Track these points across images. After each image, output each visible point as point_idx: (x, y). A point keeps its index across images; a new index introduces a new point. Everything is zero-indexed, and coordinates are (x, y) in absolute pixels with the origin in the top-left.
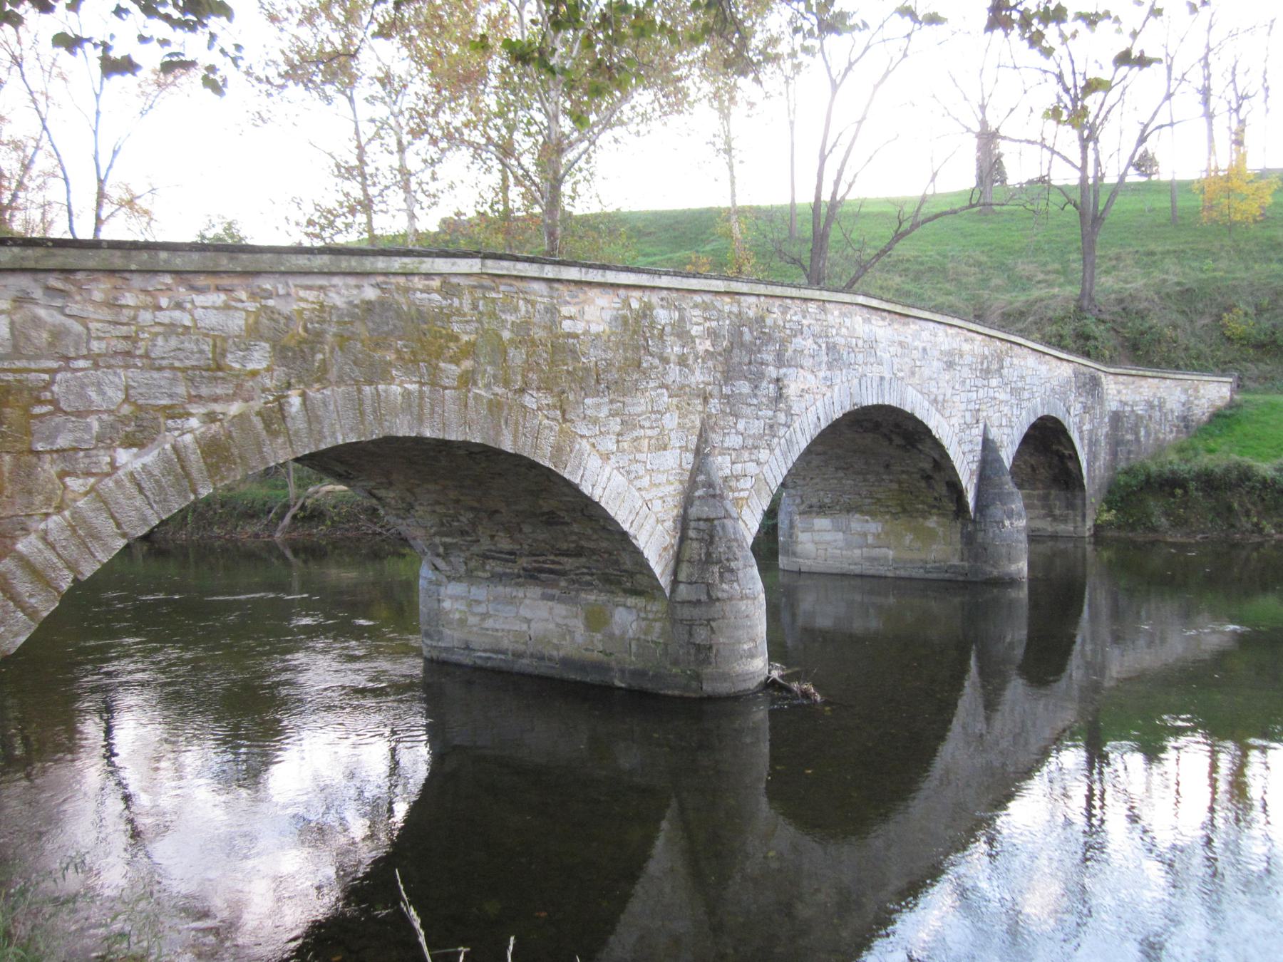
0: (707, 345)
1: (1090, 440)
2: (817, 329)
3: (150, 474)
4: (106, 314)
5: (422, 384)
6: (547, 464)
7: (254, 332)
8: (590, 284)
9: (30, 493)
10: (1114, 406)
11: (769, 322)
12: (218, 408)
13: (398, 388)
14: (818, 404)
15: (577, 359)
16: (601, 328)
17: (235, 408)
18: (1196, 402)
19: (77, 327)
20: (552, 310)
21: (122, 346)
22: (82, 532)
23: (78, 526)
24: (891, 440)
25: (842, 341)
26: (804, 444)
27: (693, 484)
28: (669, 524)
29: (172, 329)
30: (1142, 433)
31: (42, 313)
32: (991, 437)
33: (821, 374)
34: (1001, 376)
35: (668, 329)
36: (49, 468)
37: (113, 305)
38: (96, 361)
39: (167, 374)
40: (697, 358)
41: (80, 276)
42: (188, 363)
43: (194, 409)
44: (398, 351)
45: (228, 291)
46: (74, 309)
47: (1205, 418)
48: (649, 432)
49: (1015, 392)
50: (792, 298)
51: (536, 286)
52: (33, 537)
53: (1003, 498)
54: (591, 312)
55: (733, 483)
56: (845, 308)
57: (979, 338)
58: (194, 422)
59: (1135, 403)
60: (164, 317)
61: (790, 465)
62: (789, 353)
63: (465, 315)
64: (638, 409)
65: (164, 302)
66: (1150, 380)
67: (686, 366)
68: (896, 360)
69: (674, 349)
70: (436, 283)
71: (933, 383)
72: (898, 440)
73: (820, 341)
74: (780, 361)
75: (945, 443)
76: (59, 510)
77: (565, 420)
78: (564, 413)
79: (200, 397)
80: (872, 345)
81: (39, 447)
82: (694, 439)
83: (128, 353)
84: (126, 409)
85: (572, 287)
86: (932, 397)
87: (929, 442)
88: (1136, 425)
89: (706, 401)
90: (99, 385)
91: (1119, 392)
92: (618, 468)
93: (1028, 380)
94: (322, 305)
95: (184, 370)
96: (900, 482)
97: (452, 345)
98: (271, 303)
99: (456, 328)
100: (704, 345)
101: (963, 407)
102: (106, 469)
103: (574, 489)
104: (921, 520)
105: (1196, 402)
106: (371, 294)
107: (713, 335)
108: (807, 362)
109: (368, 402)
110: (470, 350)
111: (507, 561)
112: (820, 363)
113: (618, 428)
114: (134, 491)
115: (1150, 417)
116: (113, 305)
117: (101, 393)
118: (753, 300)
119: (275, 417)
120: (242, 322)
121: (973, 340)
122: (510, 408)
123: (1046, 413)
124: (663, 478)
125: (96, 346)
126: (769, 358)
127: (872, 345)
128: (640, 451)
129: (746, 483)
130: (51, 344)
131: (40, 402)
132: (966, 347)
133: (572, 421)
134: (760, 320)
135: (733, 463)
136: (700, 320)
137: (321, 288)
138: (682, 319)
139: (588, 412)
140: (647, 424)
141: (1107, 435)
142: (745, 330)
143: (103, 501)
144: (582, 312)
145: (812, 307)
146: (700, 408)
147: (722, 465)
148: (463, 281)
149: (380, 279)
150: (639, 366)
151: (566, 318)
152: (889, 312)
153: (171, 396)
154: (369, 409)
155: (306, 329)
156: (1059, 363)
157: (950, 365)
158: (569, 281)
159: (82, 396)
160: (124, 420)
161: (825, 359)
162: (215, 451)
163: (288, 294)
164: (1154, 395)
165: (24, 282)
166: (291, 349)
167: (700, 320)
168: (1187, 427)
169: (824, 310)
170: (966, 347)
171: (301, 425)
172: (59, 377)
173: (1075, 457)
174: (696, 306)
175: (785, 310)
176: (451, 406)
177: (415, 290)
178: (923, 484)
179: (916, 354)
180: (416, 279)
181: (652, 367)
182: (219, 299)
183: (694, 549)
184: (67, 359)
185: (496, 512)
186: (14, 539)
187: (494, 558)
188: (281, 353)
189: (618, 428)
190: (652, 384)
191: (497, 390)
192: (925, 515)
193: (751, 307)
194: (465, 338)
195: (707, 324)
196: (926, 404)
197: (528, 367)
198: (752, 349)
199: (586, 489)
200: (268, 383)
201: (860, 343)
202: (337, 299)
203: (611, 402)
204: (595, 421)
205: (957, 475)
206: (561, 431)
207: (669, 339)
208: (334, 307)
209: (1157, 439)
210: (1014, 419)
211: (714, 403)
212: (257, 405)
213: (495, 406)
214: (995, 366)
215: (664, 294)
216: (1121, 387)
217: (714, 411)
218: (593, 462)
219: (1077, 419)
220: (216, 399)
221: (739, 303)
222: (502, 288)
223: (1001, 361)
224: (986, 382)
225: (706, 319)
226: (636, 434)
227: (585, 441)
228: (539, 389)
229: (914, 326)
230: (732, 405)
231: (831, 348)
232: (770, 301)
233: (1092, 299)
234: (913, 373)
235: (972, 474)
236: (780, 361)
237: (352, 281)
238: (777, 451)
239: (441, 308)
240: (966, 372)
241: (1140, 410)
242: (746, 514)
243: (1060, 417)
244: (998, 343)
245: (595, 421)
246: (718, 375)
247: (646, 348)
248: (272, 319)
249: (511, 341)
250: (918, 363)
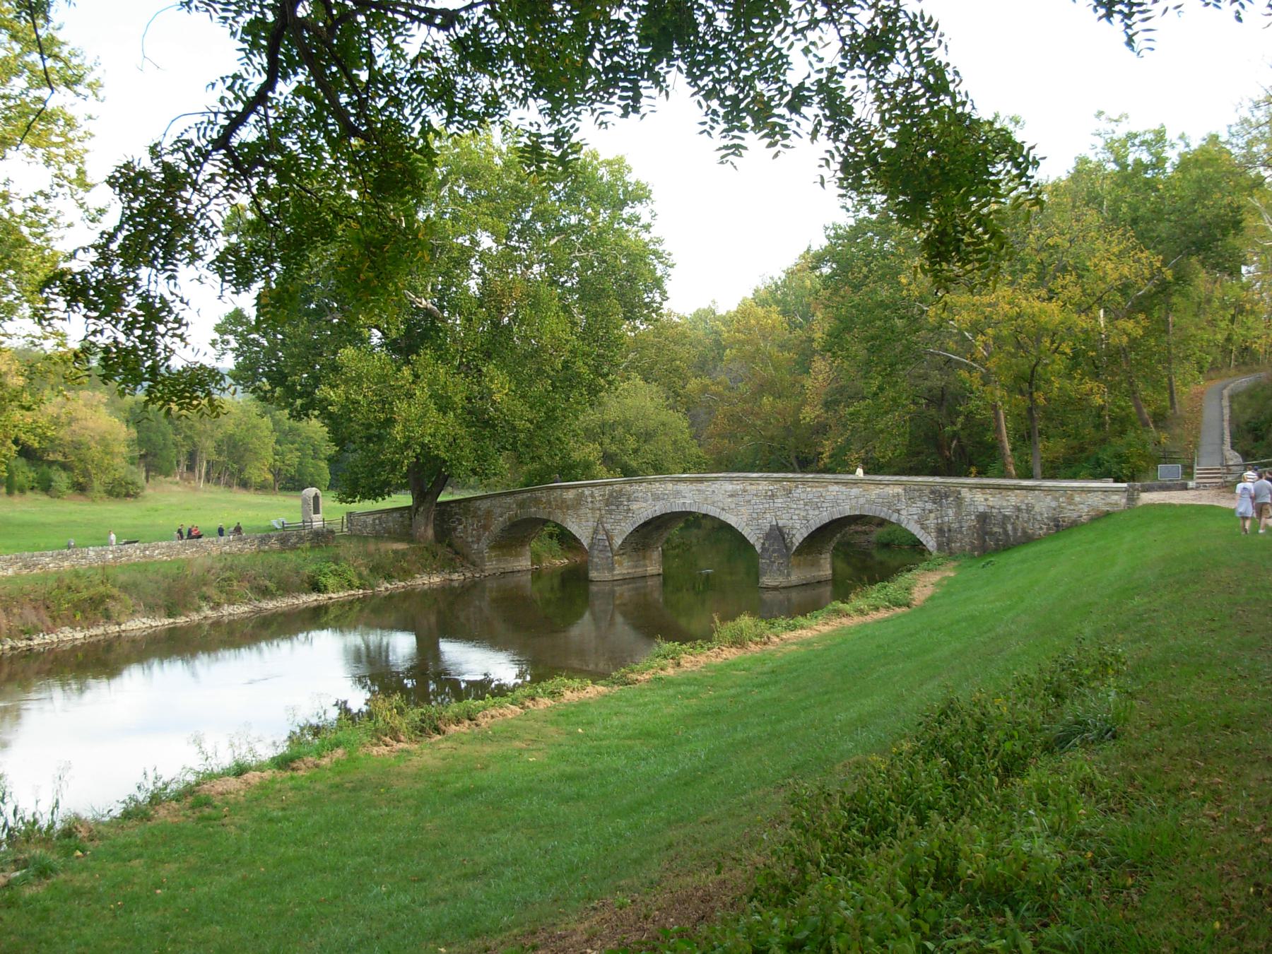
1: (940, 531)
10: (981, 509)
13: (533, 509)
30: (1009, 527)
69: (590, 499)
75: (733, 524)
88: (1004, 523)
91: (986, 500)
115: (1017, 517)
119: (516, 514)
123: (857, 513)
134: (621, 490)
145: (644, 484)
162: (509, 519)
164: (1022, 502)
170: (749, 488)
193: (616, 487)
209: (1024, 532)
211: (603, 512)
216: (988, 496)
219: (916, 517)
230: (610, 512)
235: (758, 538)
242: (615, 538)
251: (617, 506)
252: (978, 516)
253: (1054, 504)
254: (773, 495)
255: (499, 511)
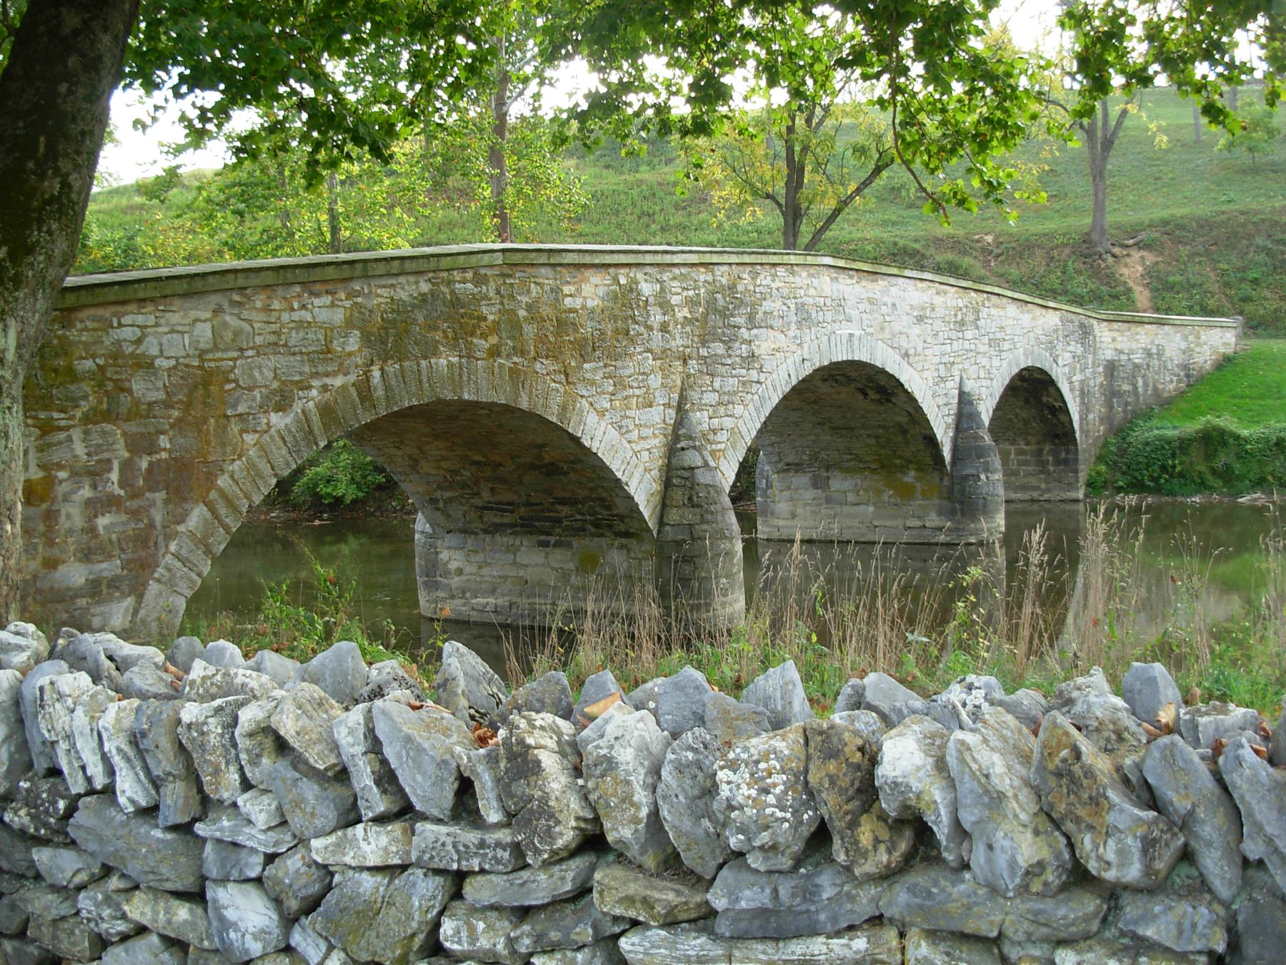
0: (686, 312)
1: (1082, 391)
2: (785, 292)
3: (290, 431)
4: (262, 316)
5: (461, 357)
6: (555, 420)
7: (349, 323)
8: (586, 266)
9: (224, 445)
10: (1109, 355)
11: (740, 288)
12: (328, 381)
13: (444, 361)
14: (789, 361)
15: (576, 331)
16: (596, 303)
17: (338, 381)
18: (1197, 349)
19: (247, 327)
20: (556, 291)
21: (272, 338)
22: (254, 473)
23: (251, 465)
24: (865, 394)
25: (810, 301)
26: (775, 400)
27: (676, 437)
28: (655, 473)
29: (301, 324)
30: (1140, 382)
31: (228, 318)
32: (967, 389)
33: (791, 334)
34: (977, 328)
35: (651, 300)
36: (234, 428)
37: (267, 309)
38: (259, 351)
39: (298, 358)
40: (676, 323)
41: (248, 291)
42: (311, 349)
43: (315, 383)
44: (444, 332)
45: (333, 293)
46: (245, 314)
47: (1208, 366)
48: (637, 392)
49: (994, 343)
50: (761, 264)
51: (543, 271)
52: (226, 476)
53: (981, 452)
54: (587, 289)
55: (711, 437)
56: (812, 270)
57: (953, 290)
58: (314, 392)
59: (1132, 352)
60: (296, 316)
61: (763, 420)
62: (760, 316)
63: (490, 299)
64: (628, 372)
65: (296, 305)
66: (1147, 326)
67: (667, 332)
68: (864, 315)
69: (657, 317)
70: (469, 275)
71: (904, 337)
72: (872, 395)
73: (788, 302)
74: (752, 322)
75: (918, 395)
76: (240, 457)
77: (568, 383)
78: (567, 375)
79: (317, 373)
80: (840, 304)
81: (229, 413)
82: (676, 396)
83: (276, 344)
84: (275, 385)
85: (572, 270)
86: (903, 351)
87: (901, 394)
88: (1134, 377)
89: (685, 362)
90: (260, 367)
91: (1114, 340)
92: (612, 424)
93: (1008, 331)
94: (392, 299)
95: (308, 354)
96: (877, 437)
97: (483, 324)
98: (359, 300)
99: (485, 310)
100: (684, 313)
101: (937, 360)
102: (265, 427)
103: (576, 440)
104: (899, 475)
105: (1197, 349)
106: (425, 287)
107: (692, 303)
108: (777, 323)
109: (424, 372)
110: (496, 327)
111: (505, 511)
112: (789, 324)
113: (611, 389)
114: (280, 443)
115: (1148, 365)
116: (267, 309)
117: (261, 373)
118: (725, 268)
119: (364, 388)
120: (342, 316)
121: (945, 293)
122: (526, 373)
124: (649, 432)
125: (259, 340)
126: (740, 320)
127: (840, 304)
128: (630, 409)
129: (722, 437)
130: (233, 340)
131: (229, 381)
132: (938, 300)
133: (574, 384)
134: (732, 287)
135: (710, 418)
136: (679, 290)
137: (392, 286)
138: (662, 290)
139: (587, 376)
140: (635, 385)
141: (1101, 385)
142: (719, 296)
143: (263, 449)
144: (579, 290)
145: (781, 271)
146: (680, 369)
147: (701, 419)
148: (489, 272)
149: (431, 275)
150: (627, 334)
151: (567, 296)
152: (857, 270)
153: (300, 374)
154: (425, 380)
155: (383, 319)
156: (1044, 311)
157: (920, 319)
158: (569, 265)
159: (251, 376)
160: (274, 393)
161: (794, 319)
162: (326, 411)
163: (370, 292)
164: (1152, 342)
165: (215, 299)
166: (373, 334)
167: (679, 290)
168: (1188, 376)
169: (793, 273)
171: (380, 392)
172: (238, 362)
173: (1066, 411)
174: (675, 278)
175: (755, 276)
176: (481, 374)
177: (455, 282)
178: (900, 438)
179: (884, 310)
180: (455, 273)
181: (639, 334)
182: (327, 300)
183: (678, 496)
184: (242, 350)
185: (500, 465)
186: (216, 476)
187: (492, 509)
188: (366, 339)
189: (611, 389)
190: (639, 350)
191: (515, 359)
192: (903, 469)
193: (722, 276)
194: (491, 318)
195: (685, 293)
196: (898, 358)
197: (541, 339)
198: (724, 314)
199: (586, 442)
200: (360, 361)
201: (829, 302)
202: (403, 295)
203: (605, 366)
204: (593, 383)
205: (931, 429)
206: (566, 391)
207: (652, 310)
208: (400, 300)
209: (1155, 389)
210: (993, 371)
212: (352, 378)
213: (514, 372)
214: (972, 318)
215: (648, 269)
216: (1116, 334)
217: (692, 371)
218: (592, 418)
219: (1066, 370)
220: (327, 375)
221: (712, 272)
222: (518, 275)
223: (977, 312)
224: (960, 335)
225: (684, 289)
226: (626, 393)
227: (584, 401)
228: (547, 358)
229: (882, 283)
231: (801, 308)
232: (741, 268)
233: (1103, 232)
234: (882, 329)
235: (948, 426)
236: (752, 322)
237: (412, 279)
238: (751, 407)
239: (474, 295)
240: (938, 325)
241: (1138, 358)
242: (724, 465)
243: (1047, 368)
244: (973, 294)
245: (593, 383)
246: (696, 339)
247: (633, 317)
248: (360, 312)
249: (526, 319)
250: (888, 319)
251: (728, 344)
252: (1105, 367)
253: (1183, 345)
254: (962, 323)
255: (266, 371)
